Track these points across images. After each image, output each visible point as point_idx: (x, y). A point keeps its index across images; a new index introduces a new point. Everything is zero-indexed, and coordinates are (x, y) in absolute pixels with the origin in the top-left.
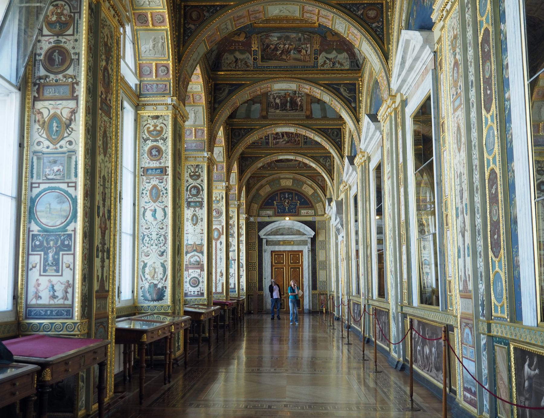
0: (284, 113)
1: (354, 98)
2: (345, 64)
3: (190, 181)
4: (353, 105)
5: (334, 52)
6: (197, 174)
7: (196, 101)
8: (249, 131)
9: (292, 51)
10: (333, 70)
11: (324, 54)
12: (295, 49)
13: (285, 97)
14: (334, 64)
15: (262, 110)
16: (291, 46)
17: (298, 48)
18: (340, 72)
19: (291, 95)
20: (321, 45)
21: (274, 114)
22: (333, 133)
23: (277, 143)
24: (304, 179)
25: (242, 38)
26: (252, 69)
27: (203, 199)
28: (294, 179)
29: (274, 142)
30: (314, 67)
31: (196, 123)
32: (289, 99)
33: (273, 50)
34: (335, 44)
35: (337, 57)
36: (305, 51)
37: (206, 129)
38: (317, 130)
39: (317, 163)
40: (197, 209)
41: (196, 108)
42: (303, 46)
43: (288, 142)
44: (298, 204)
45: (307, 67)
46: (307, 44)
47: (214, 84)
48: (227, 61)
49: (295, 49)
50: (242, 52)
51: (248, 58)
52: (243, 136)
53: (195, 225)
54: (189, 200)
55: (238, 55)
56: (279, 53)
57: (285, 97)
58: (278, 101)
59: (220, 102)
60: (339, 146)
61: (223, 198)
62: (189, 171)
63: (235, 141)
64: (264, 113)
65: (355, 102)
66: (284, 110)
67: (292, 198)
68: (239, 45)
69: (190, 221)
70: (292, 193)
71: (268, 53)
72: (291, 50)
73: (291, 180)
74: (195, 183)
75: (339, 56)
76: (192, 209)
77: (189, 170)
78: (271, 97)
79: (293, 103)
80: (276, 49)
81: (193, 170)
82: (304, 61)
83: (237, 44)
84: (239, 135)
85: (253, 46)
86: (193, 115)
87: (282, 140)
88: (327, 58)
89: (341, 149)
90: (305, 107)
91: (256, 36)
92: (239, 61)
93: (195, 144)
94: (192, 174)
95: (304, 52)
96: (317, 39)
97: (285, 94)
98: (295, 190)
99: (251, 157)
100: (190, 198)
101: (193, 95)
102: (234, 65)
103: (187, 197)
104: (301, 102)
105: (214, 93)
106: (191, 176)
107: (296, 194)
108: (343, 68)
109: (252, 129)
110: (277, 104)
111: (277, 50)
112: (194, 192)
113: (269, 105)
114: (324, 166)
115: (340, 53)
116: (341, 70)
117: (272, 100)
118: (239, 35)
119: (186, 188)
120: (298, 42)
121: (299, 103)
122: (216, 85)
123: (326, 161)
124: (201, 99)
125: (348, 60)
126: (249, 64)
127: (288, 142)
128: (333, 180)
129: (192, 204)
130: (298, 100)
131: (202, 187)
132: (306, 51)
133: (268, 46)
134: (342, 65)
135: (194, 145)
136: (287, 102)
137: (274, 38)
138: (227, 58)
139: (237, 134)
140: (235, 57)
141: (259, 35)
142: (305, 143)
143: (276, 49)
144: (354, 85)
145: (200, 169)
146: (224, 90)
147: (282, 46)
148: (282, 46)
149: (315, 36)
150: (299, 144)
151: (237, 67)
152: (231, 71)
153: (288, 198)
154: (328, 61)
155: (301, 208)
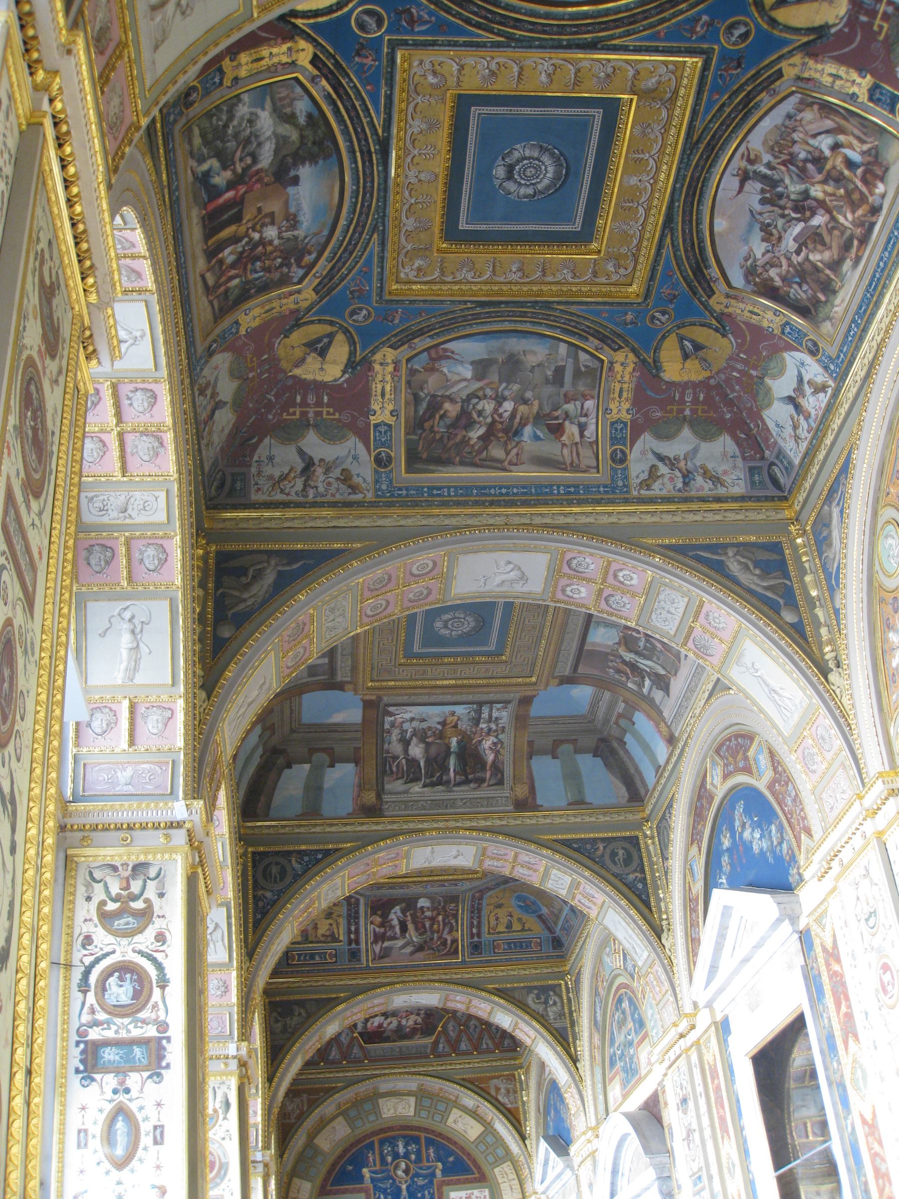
0: (439, 793)
1: (790, 599)
2: (728, 479)
3: (102, 938)
4: (789, 617)
5: (686, 432)
6: (139, 905)
7: (140, 573)
8: (318, 861)
9: (528, 430)
10: (686, 500)
11: (647, 441)
12: (538, 418)
13: (441, 735)
14: (687, 477)
15: (362, 787)
16: (522, 408)
17: (548, 416)
18: (716, 506)
19: (464, 725)
20: (639, 400)
21: (403, 797)
22: (614, 854)
23: (386, 953)
24: (452, 1089)
25: (331, 369)
26: (370, 496)
27: (163, 1027)
28: (421, 1095)
29: (377, 948)
30: (611, 488)
31: (139, 679)
32: (454, 741)
33: (454, 425)
34: (688, 399)
35: (695, 451)
36: (575, 430)
37: (181, 703)
38: (558, 846)
39: (519, 1012)
40: (134, 1080)
41: (140, 608)
42: (570, 407)
43: (420, 948)
44: (438, 1173)
45: (587, 488)
46: (585, 397)
47: (218, 553)
48: (268, 470)
49: (538, 418)
50: (331, 434)
51: (355, 458)
52: (297, 877)
53: (121, 1164)
54: (94, 1034)
55: (313, 444)
56: (476, 434)
57: (441, 735)
58: (417, 751)
59: (242, 620)
60: (639, 897)
61: (227, 1105)
62: (99, 894)
63: (269, 895)
64: (370, 797)
65: (792, 604)
66: (440, 783)
67: (418, 1153)
68: (319, 403)
69: (95, 1143)
70: (416, 1140)
71: (435, 436)
72: (523, 425)
73: (412, 1100)
74: (124, 951)
75: (705, 446)
76: (110, 1081)
77: (98, 888)
78: (395, 735)
79: (471, 763)
80: (465, 420)
81: (115, 889)
82: (575, 468)
83: (311, 399)
84: (283, 873)
85: (375, 406)
86: (126, 639)
87: (400, 943)
88: (661, 458)
89: (647, 905)
90: (508, 771)
91: (389, 354)
92: (319, 471)
93: (129, 772)
94: (111, 906)
95: (572, 430)
96: (624, 365)
97: (444, 723)
98: (426, 1130)
99: (301, 1003)
100: (96, 1024)
101: (128, 543)
102: (299, 484)
103: (86, 1018)
104: (497, 753)
105: (218, 585)
106: (105, 918)
107: (430, 1142)
108: (721, 491)
109: (327, 853)
110: (413, 763)
111: (470, 424)
112: (120, 992)
113: (385, 766)
114: (541, 1019)
115: (706, 436)
116: (718, 500)
117: (396, 748)
118: (322, 353)
119: (77, 975)
120: (549, 390)
121: (490, 757)
122: (223, 557)
123: (546, 1002)
124: (163, 562)
125: (740, 462)
126: (356, 480)
127: (420, 948)
128: (575, 1060)
129: (109, 1055)
130: (487, 743)
131: (159, 967)
132: (582, 428)
133: (435, 405)
134: (716, 480)
135: (124, 775)
136: (448, 753)
137: (462, 363)
138: (271, 458)
139: (275, 870)
140: (301, 453)
141: (404, 352)
142: (476, 948)
143: (465, 420)
144: (776, 548)
145: (151, 885)
146: (258, 575)
147: (488, 406)
148: (488, 406)
149: (620, 356)
150: (456, 952)
151: (311, 493)
152: (285, 505)
153: (406, 1156)
154: (663, 469)
155: (449, 1183)
